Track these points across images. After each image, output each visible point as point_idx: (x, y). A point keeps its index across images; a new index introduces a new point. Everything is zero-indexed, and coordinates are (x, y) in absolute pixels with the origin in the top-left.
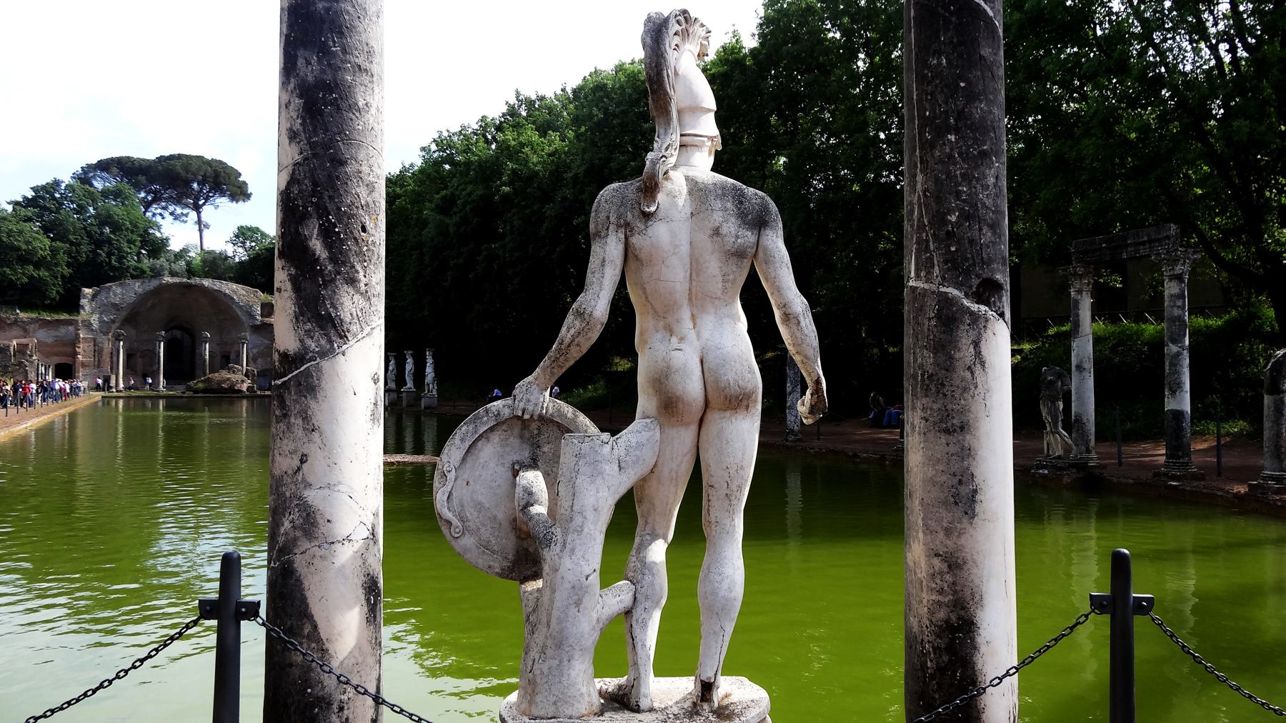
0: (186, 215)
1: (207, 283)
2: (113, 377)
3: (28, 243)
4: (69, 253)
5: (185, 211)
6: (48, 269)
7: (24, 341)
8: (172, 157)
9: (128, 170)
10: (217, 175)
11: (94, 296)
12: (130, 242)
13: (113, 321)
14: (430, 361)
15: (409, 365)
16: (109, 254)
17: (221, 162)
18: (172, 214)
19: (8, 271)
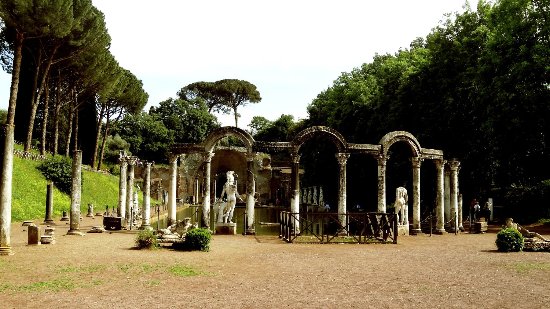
0: (230, 110)
1: (237, 149)
2: (194, 197)
3: (158, 131)
4: (175, 135)
5: (229, 108)
6: (167, 143)
7: (157, 179)
8: (222, 82)
9: (202, 89)
10: (244, 89)
11: (186, 157)
12: (203, 128)
13: (194, 169)
14: (321, 191)
15: (315, 193)
16: (193, 135)
17: (246, 82)
18: (223, 110)
19: (150, 145)
